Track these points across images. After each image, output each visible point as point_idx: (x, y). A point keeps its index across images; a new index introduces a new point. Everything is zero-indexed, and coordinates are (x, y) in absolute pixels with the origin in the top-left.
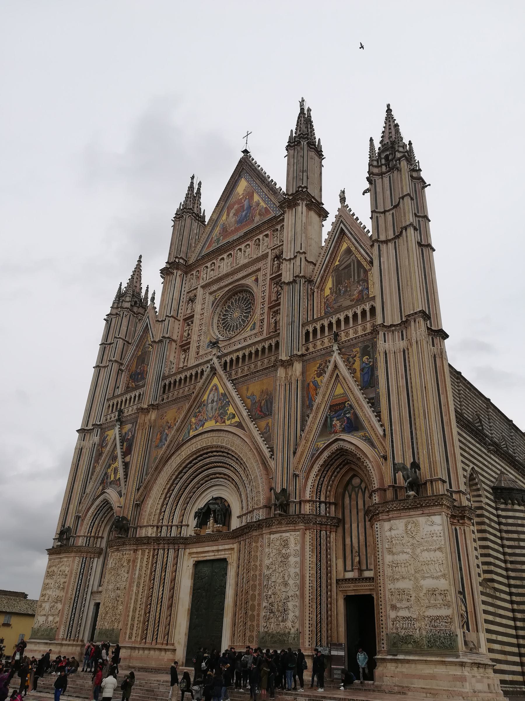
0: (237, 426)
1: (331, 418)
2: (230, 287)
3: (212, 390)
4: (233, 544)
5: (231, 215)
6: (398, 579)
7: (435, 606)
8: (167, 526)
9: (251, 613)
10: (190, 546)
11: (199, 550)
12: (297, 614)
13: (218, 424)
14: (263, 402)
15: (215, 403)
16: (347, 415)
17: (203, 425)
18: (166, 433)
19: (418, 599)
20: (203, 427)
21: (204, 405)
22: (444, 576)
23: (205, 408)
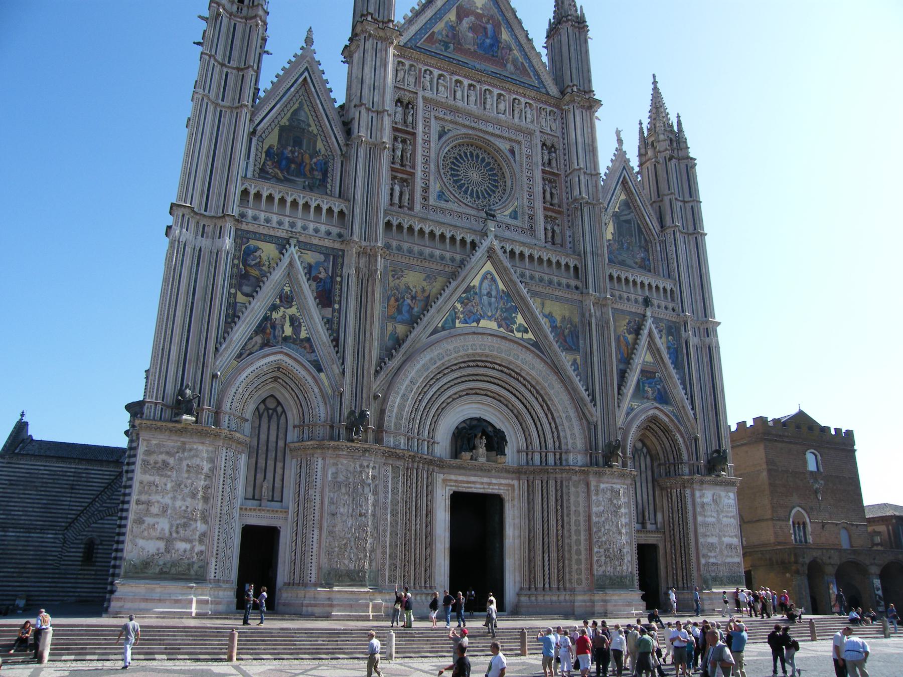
0: (532, 345)
1: (643, 383)
2: (470, 132)
3: (484, 277)
4: (512, 479)
6: (709, 536)
7: (731, 556)
9: (576, 557)
10: (446, 470)
11: (461, 478)
12: (630, 559)
13: (501, 329)
14: (567, 331)
15: (493, 299)
16: (658, 387)
17: (478, 321)
18: (409, 305)
19: (721, 551)
22: (736, 536)
23: (477, 297)
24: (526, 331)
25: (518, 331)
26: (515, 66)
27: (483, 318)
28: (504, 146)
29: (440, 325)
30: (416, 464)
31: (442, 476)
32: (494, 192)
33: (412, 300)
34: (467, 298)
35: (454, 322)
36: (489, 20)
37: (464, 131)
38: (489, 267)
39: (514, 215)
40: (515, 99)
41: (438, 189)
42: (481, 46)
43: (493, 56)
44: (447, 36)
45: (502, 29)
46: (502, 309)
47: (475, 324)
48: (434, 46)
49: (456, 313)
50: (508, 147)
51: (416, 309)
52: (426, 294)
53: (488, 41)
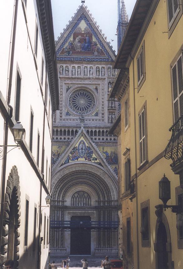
3: (80, 143)
5: (77, 40)
8: (57, 201)
13: (87, 160)
14: (113, 157)
15: (83, 150)
17: (77, 159)
20: (77, 160)
21: (77, 149)
24: (96, 159)
25: (93, 160)
26: (98, 52)
27: (80, 158)
28: (92, 88)
29: (63, 163)
30: (56, 209)
31: (67, 212)
32: (90, 106)
33: (53, 156)
34: (74, 152)
35: (69, 161)
36: (87, 35)
37: (77, 86)
38: (82, 139)
39: (97, 115)
40: (97, 67)
41: (66, 112)
42: (83, 48)
43: (88, 51)
44: (69, 48)
45: (93, 37)
46: (87, 153)
47: (76, 160)
48: (64, 55)
49: (69, 157)
50: (95, 87)
51: (55, 159)
52: (58, 153)
53: (86, 45)
